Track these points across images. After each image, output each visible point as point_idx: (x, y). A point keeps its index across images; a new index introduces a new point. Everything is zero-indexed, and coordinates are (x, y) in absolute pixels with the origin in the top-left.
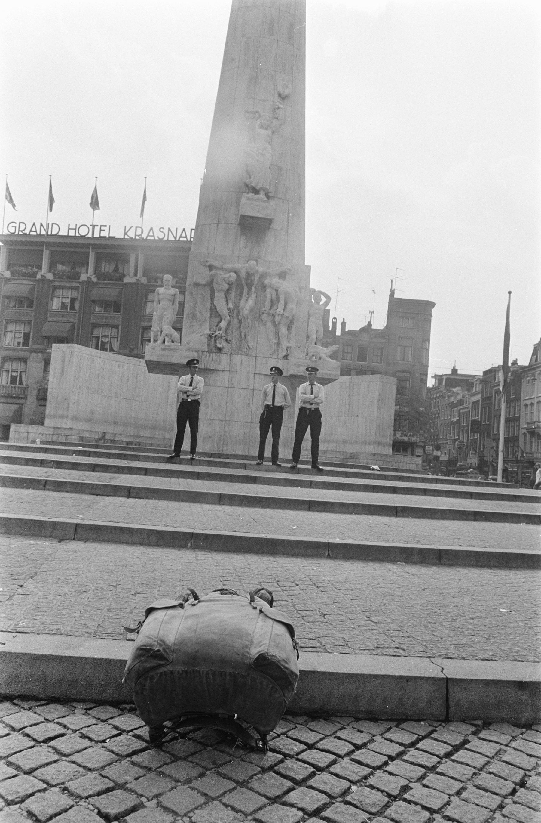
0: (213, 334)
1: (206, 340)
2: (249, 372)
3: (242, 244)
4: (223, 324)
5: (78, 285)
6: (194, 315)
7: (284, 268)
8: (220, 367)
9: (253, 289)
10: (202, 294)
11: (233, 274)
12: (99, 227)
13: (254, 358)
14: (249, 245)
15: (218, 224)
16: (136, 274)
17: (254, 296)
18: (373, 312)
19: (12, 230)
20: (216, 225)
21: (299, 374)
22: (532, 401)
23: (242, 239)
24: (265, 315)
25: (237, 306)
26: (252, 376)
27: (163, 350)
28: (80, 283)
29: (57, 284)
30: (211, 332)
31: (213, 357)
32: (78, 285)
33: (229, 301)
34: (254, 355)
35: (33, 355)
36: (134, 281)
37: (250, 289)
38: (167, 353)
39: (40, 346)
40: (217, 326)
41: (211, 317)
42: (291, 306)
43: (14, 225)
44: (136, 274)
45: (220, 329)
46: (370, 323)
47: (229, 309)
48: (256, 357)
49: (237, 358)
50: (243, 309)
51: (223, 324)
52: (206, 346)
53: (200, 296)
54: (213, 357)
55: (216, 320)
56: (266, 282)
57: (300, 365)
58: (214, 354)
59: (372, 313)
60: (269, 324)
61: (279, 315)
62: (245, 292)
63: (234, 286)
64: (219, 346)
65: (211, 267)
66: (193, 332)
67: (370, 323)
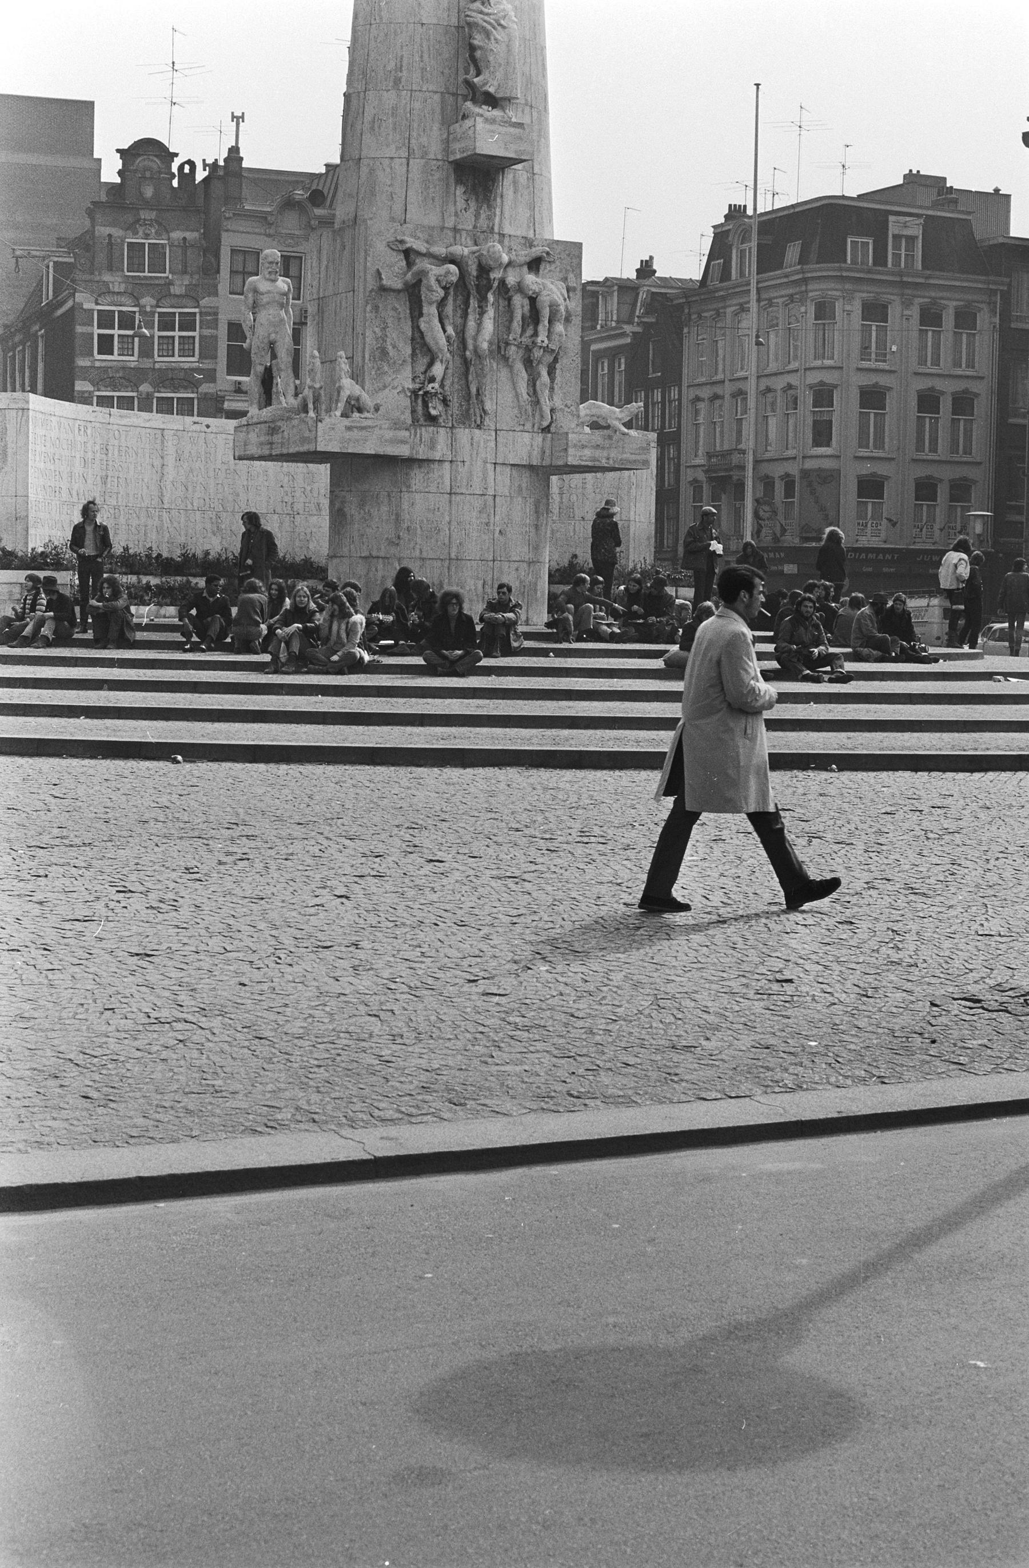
0: (420, 389)
1: (407, 402)
2: (485, 462)
3: (461, 204)
6: (384, 352)
7: (536, 251)
8: (437, 456)
9: (491, 297)
10: (395, 309)
11: (453, 268)
13: (494, 434)
14: (473, 204)
15: (408, 159)
17: (491, 312)
18: (243, 117)
20: (404, 161)
21: (583, 463)
22: (718, 389)
23: (458, 193)
24: (513, 348)
25: (461, 333)
26: (490, 467)
27: (349, 428)
30: (417, 386)
31: (421, 434)
33: (446, 322)
34: (493, 428)
37: (483, 299)
38: (356, 434)
40: (425, 372)
41: (414, 355)
45: (432, 380)
46: (234, 151)
47: (448, 339)
48: (496, 431)
49: (463, 434)
50: (475, 339)
51: (438, 370)
52: (408, 412)
53: (391, 313)
54: (421, 434)
55: (423, 362)
57: (583, 447)
58: (423, 429)
59: (238, 119)
60: (519, 366)
61: (541, 347)
62: (473, 303)
63: (451, 291)
64: (433, 412)
66: (385, 387)
67: (234, 151)
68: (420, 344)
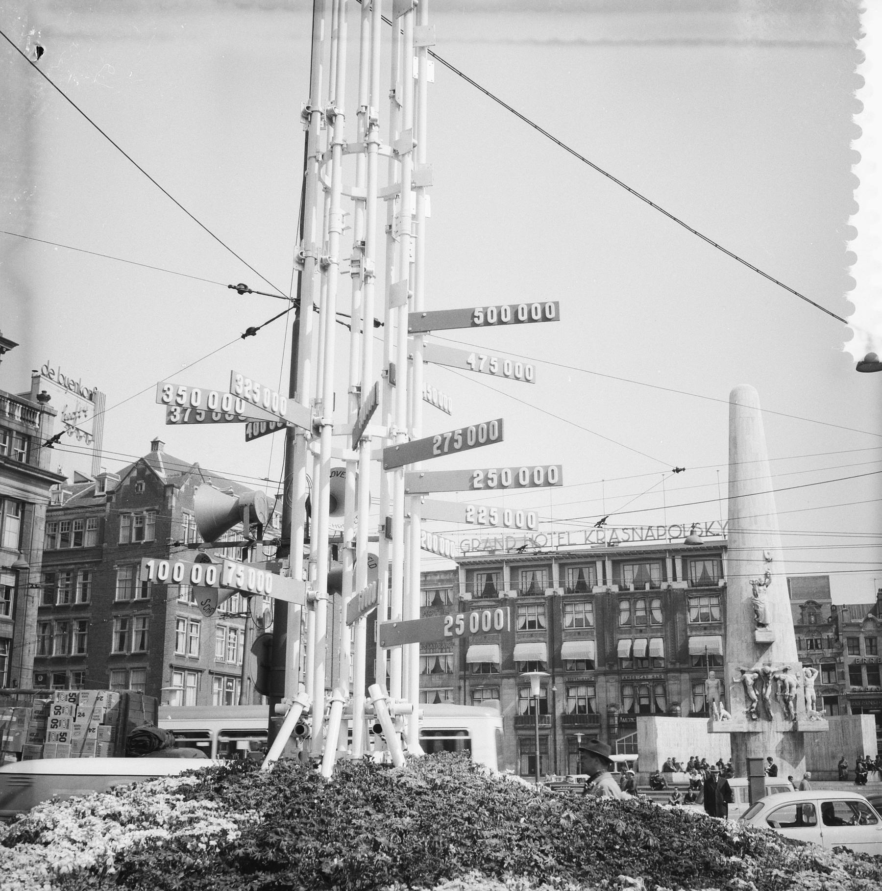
4: (755, 705)
5: (543, 601)
12: (557, 535)
16: (605, 583)
19: (466, 549)
28: (544, 598)
29: (519, 602)
32: (543, 601)
35: (505, 681)
36: (604, 591)
39: (511, 671)
42: (794, 689)
43: (466, 542)
44: (605, 583)
51: (755, 705)
56: (777, 676)
65: (743, 672)
68: (748, 698)
